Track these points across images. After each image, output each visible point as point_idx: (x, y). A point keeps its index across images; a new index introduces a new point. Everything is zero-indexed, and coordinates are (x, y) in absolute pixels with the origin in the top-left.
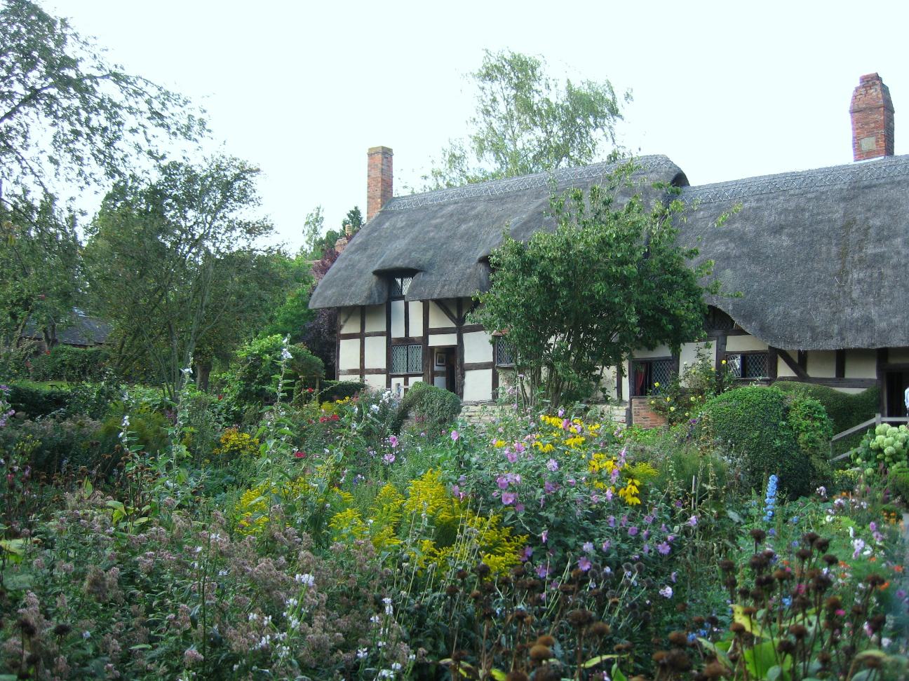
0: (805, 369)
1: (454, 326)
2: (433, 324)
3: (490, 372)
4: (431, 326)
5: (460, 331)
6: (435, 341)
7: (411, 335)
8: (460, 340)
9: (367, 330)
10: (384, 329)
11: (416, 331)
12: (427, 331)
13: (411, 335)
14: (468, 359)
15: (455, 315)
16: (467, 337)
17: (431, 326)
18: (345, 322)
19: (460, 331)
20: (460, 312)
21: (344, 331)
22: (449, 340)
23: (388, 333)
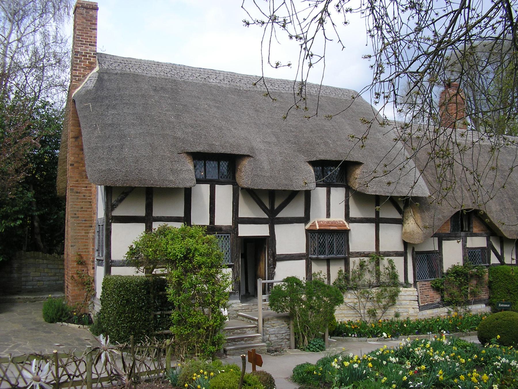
0: (503, 258)
1: (266, 216)
2: (244, 212)
3: (303, 263)
4: (240, 215)
5: (272, 221)
6: (246, 231)
7: (218, 222)
8: (272, 231)
9: (156, 213)
10: (182, 215)
11: (224, 218)
12: (237, 220)
13: (217, 223)
14: (280, 250)
15: (268, 206)
16: (279, 229)
17: (240, 215)
18: (120, 201)
19: (272, 221)
20: (272, 204)
21: (117, 212)
22: (261, 231)
23: (187, 219)
